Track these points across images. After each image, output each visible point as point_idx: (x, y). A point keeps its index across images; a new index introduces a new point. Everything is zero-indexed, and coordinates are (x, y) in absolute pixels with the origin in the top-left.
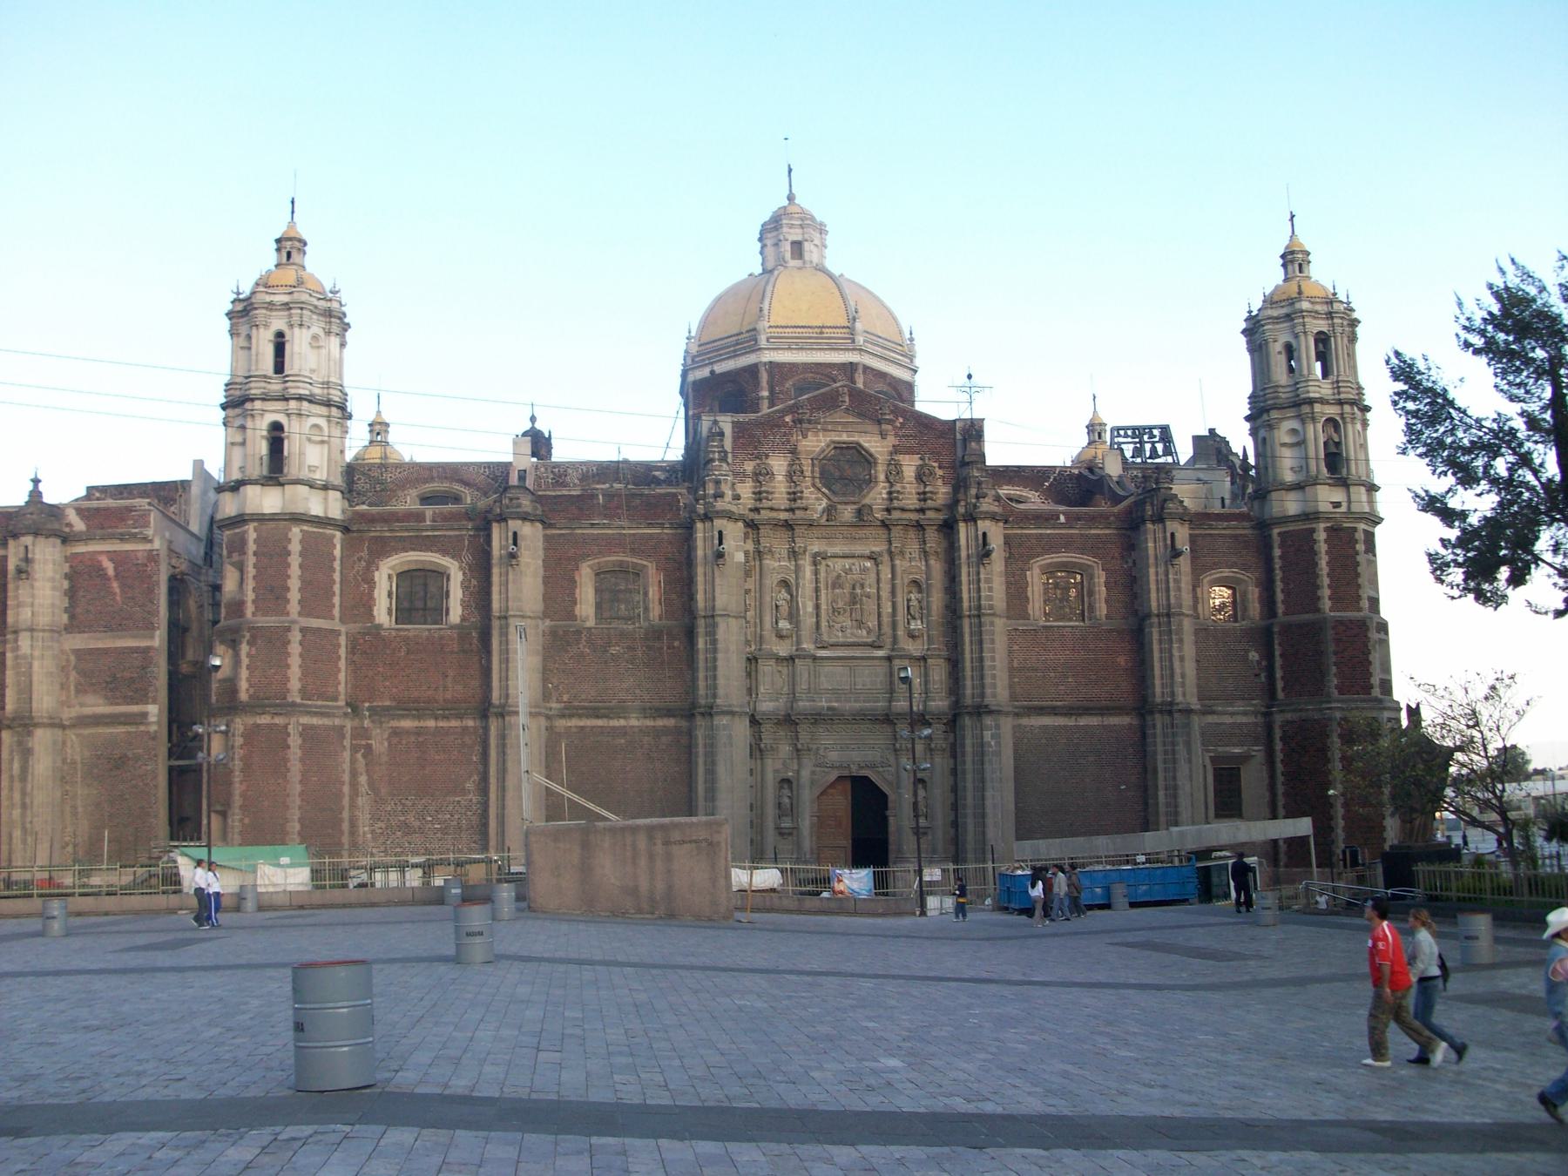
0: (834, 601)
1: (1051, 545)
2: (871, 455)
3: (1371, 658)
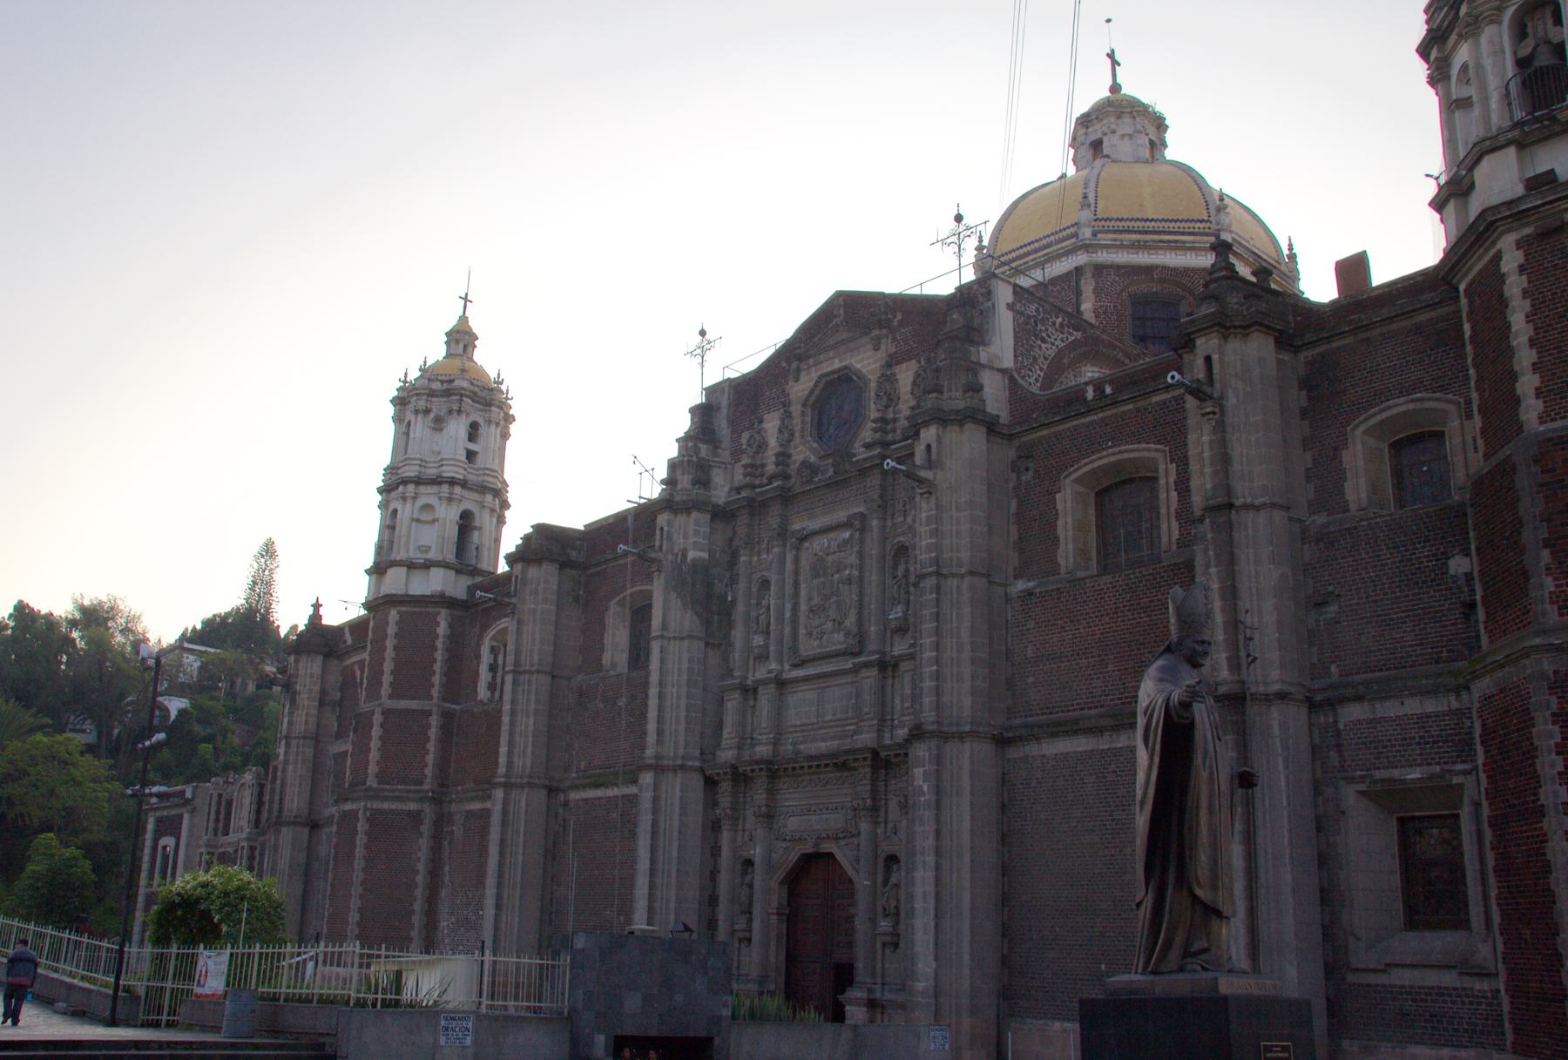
0: (810, 599)
2: (861, 377)
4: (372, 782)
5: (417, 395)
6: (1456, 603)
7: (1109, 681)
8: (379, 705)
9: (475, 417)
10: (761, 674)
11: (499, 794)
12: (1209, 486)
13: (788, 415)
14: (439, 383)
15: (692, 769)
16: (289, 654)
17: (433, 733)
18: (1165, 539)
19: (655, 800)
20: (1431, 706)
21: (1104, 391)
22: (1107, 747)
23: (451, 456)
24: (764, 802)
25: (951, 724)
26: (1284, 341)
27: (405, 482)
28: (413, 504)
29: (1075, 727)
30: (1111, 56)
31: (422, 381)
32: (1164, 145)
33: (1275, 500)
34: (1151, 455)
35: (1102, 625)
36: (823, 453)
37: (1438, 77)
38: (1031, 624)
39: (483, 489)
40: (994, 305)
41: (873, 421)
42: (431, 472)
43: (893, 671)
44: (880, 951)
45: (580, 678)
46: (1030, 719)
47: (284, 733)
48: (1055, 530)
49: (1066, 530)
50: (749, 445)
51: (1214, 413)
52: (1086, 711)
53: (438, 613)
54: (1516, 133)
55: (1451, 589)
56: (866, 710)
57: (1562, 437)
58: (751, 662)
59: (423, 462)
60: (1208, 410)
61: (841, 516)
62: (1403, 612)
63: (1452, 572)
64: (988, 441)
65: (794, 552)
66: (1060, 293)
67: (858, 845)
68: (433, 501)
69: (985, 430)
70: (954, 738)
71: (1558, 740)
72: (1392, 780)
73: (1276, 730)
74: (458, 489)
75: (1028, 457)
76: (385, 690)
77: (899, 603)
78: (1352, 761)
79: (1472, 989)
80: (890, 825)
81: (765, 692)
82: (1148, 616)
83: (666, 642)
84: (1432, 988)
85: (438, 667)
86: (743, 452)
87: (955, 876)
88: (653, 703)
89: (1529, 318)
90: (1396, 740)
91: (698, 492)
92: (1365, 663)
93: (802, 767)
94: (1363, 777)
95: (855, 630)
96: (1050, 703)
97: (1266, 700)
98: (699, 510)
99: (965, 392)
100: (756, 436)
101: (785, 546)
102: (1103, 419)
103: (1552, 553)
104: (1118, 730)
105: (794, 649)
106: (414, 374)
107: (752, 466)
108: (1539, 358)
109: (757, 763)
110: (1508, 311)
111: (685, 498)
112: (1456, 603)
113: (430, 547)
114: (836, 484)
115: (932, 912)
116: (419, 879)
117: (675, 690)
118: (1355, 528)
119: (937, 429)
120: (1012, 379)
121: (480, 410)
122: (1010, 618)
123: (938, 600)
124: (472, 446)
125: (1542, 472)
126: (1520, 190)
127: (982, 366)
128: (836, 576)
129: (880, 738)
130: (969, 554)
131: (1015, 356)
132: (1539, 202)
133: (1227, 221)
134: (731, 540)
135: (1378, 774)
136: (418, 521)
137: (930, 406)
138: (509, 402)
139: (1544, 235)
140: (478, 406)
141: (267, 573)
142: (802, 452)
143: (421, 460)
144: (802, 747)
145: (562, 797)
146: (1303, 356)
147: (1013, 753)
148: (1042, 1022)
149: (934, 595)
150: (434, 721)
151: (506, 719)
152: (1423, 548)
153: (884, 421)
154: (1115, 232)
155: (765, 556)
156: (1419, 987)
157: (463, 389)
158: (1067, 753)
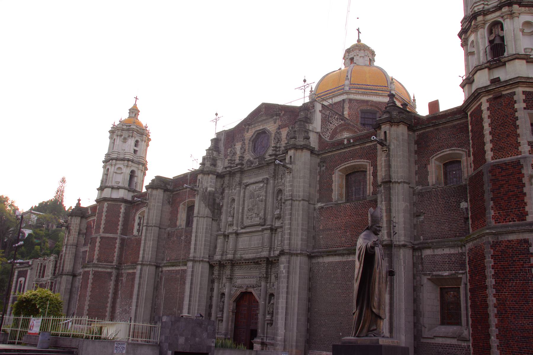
0: (248, 206)
1: (345, 158)
2: (269, 132)
3: (525, 190)
4: (95, 261)
5: (118, 130)
6: (462, 217)
7: (347, 238)
8: (99, 235)
9: (137, 138)
10: (230, 230)
11: (139, 267)
12: (383, 175)
13: (244, 143)
14: (126, 126)
15: (205, 261)
16: (69, 216)
17: (117, 245)
18: (368, 192)
19: (193, 271)
20: (453, 251)
21: (350, 141)
22: (345, 260)
23: (129, 151)
24: (229, 274)
25: (294, 250)
26: (410, 128)
27: (112, 159)
28: (115, 167)
29: (335, 253)
30: (358, 30)
31: (120, 125)
32: (374, 61)
33: (405, 181)
34: (365, 163)
35: (346, 219)
36: (255, 157)
37: (464, 44)
38: (322, 218)
39: (139, 163)
40: (315, 111)
41: (273, 147)
42: (122, 156)
43: (275, 232)
44: (266, 326)
45: (169, 229)
46: (320, 250)
47: (66, 243)
48: (332, 187)
49: (335, 187)
50: (230, 153)
51: (386, 151)
52: (339, 248)
53: (121, 205)
54: (488, 64)
55: (461, 213)
56: (266, 244)
57: (498, 165)
58: (227, 226)
59: (119, 153)
60: (384, 149)
61: (260, 178)
62: (445, 220)
63: (461, 207)
64: (311, 156)
65: (244, 190)
66: (337, 108)
67: (261, 289)
68: (122, 166)
69: (310, 152)
70: (294, 255)
71: (493, 264)
72: (439, 275)
73: (402, 257)
74: (130, 163)
75: (324, 162)
76: (102, 230)
77: (278, 208)
78: (426, 268)
79: (461, 345)
80: (272, 284)
81: (231, 236)
82: (361, 217)
83: (199, 218)
84: (449, 344)
85: (120, 223)
86: (228, 155)
87: (293, 301)
88: (193, 238)
89: (490, 125)
90: (441, 262)
91: (212, 168)
92: (432, 236)
93: (243, 263)
94: (429, 274)
95: (263, 217)
96: (327, 245)
97: (399, 247)
98: (213, 174)
99: (304, 139)
100: (233, 150)
101: (241, 188)
102: (349, 151)
103: (494, 202)
104: (350, 255)
105: (242, 223)
106: (117, 123)
107: (231, 160)
108: (492, 138)
109: (228, 260)
110: (483, 122)
111: (208, 170)
112: (462, 217)
113: (120, 182)
114: (259, 168)
115: (284, 313)
116: (110, 295)
117: (201, 235)
118: (431, 191)
119: (294, 151)
120: (320, 135)
121: (139, 136)
122: (315, 216)
123: (291, 208)
124: (136, 148)
125: (492, 176)
126: (488, 83)
127: (310, 130)
128: (257, 199)
129: (270, 254)
130: (302, 193)
131: (321, 128)
132: (494, 88)
133: (394, 87)
134: (223, 185)
135: (434, 273)
136: (116, 173)
137: (292, 143)
138: (149, 134)
139: (495, 98)
140: (139, 135)
141: (62, 188)
142: (248, 156)
143: (118, 152)
144: (243, 256)
145: (160, 269)
146: (416, 133)
147: (314, 261)
148: (319, 352)
149: (290, 207)
150: (118, 241)
151: (143, 242)
152: (452, 199)
153: (276, 147)
154: (356, 88)
155: (234, 191)
156: (444, 344)
157: (134, 129)
158: (332, 262)
